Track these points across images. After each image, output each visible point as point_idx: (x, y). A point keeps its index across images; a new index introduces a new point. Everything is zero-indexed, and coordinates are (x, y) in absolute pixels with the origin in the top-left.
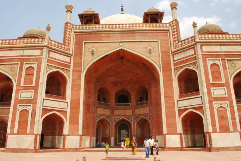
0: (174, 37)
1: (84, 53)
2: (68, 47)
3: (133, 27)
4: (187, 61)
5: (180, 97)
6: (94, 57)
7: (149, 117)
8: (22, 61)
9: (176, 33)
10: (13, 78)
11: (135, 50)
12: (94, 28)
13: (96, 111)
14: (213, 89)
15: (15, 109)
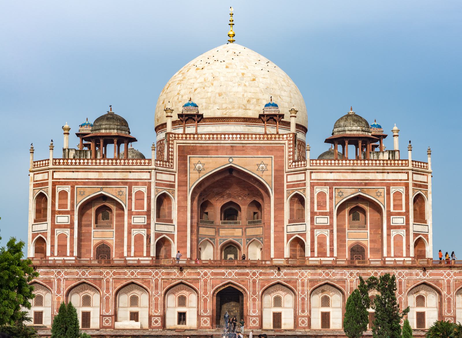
0: (289, 154)
1: (189, 170)
2: (172, 164)
3: (244, 138)
4: (298, 185)
5: (290, 222)
6: (201, 175)
7: (261, 239)
8: (130, 184)
9: (291, 150)
10: (123, 202)
11: (245, 168)
12: (200, 139)
13: (198, 231)
14: (316, 218)
15: (129, 233)
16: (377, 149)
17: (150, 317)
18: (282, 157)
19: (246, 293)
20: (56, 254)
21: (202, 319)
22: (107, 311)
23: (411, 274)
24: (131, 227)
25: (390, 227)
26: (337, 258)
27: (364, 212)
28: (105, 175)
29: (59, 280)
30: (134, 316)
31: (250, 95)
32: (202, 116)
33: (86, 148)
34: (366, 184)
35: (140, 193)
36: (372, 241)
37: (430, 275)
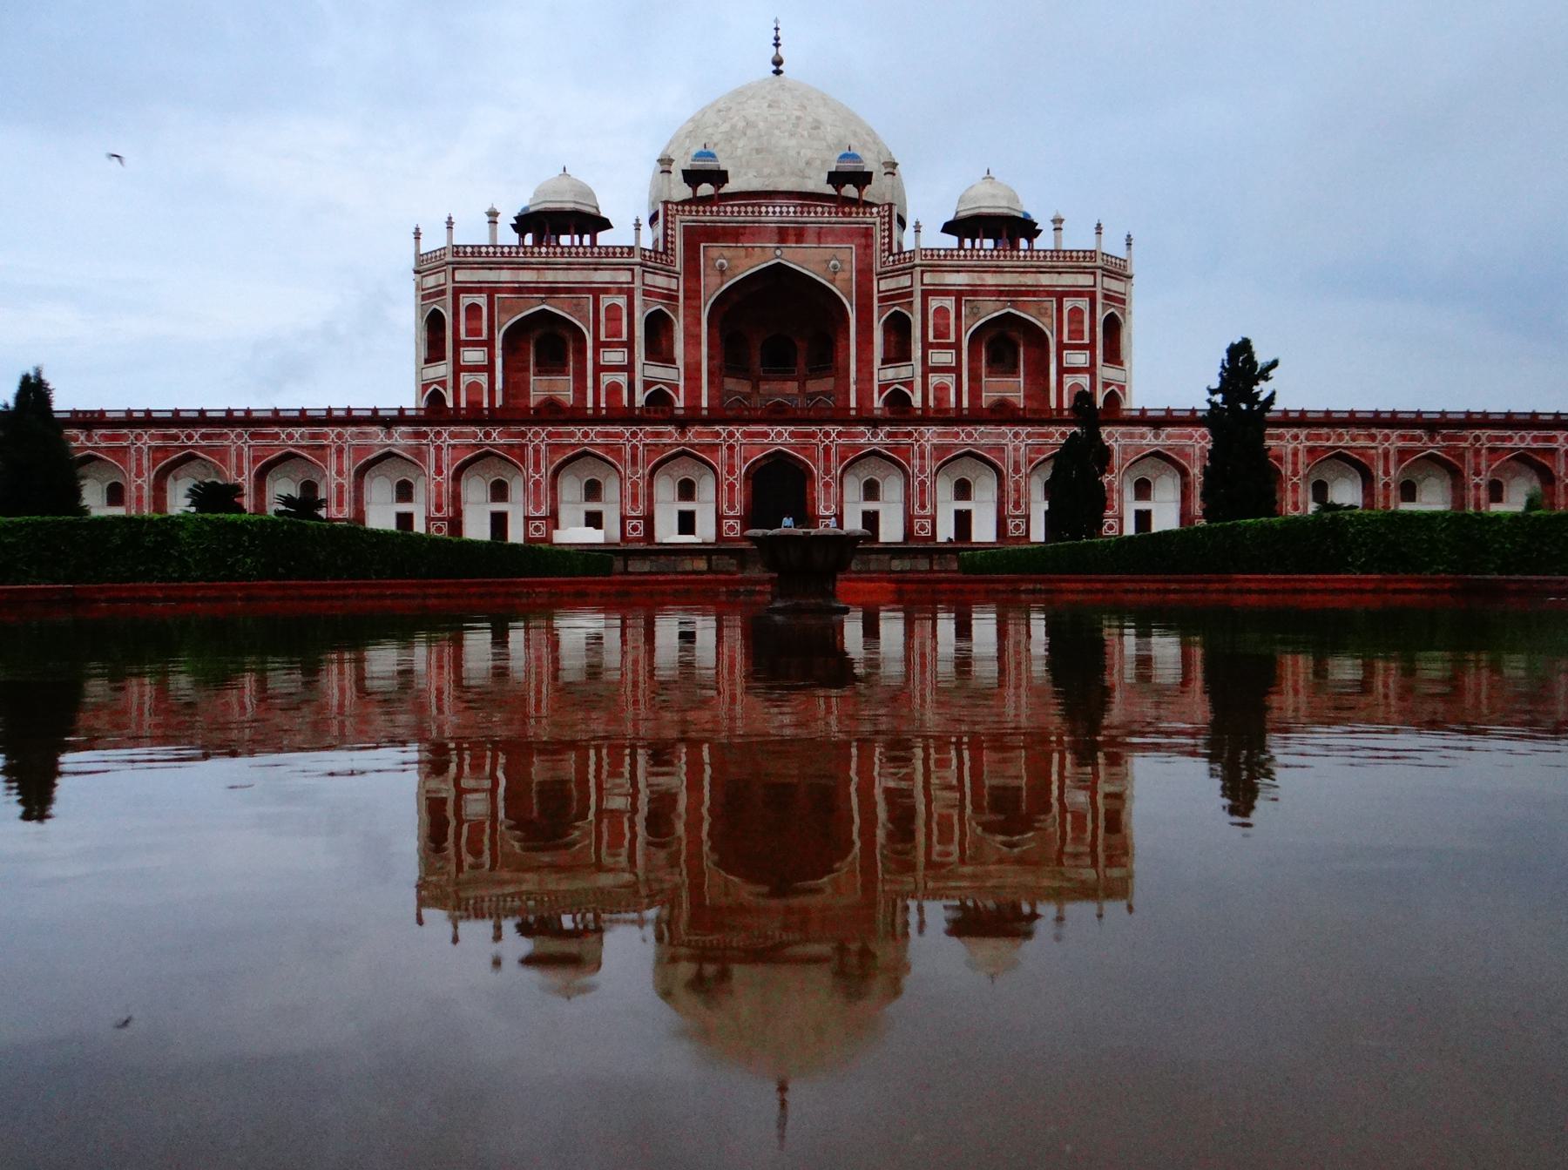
5: (884, 362)
8: (597, 292)
17: (623, 519)
18: (869, 246)
19: (811, 472)
21: (726, 523)
22: (537, 507)
23: (1131, 436)
24: (599, 369)
25: (1062, 371)
28: (550, 276)
30: (594, 520)
31: (807, 153)
35: (613, 309)
36: (1026, 397)
37: (1169, 437)
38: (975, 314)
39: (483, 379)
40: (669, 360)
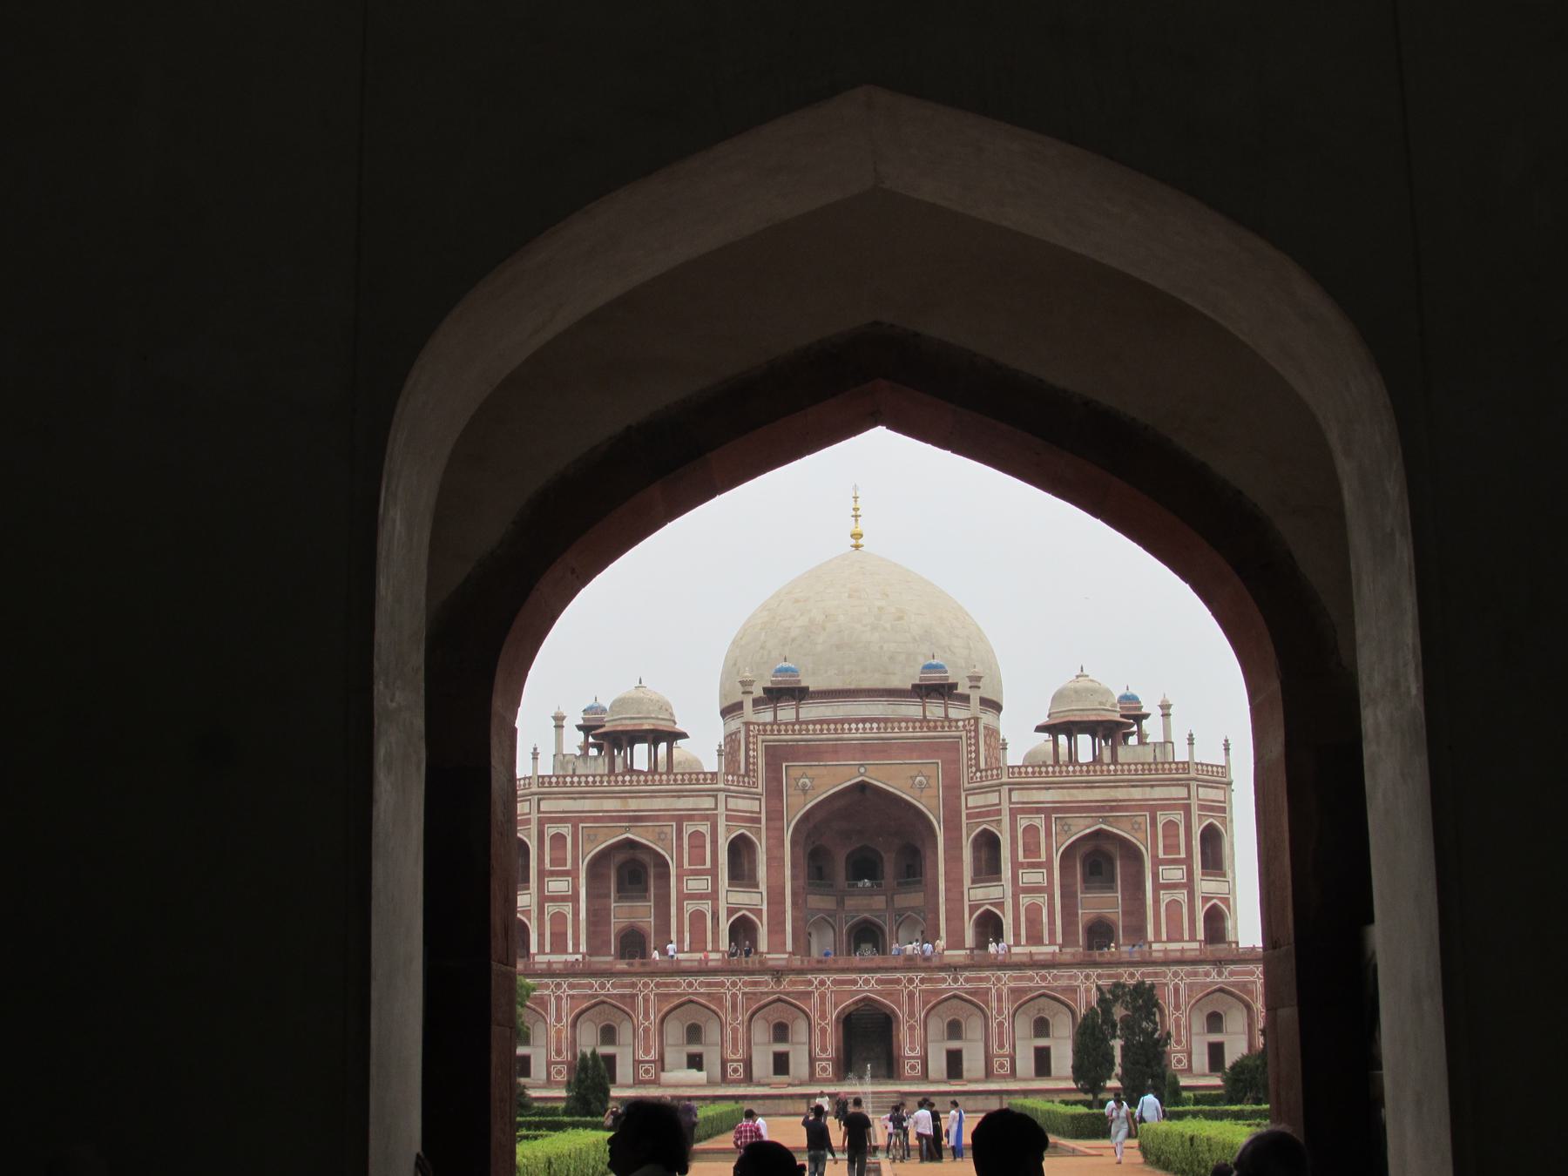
4: (988, 814)
5: (974, 882)
8: (680, 820)
13: (805, 901)
15: (680, 909)
16: (1133, 740)
17: (724, 1063)
18: (957, 761)
19: (896, 1016)
20: (548, 949)
22: (647, 1052)
23: (1196, 974)
24: (683, 897)
25: (1158, 887)
26: (1062, 947)
27: (1110, 861)
28: (633, 804)
29: (558, 998)
30: (695, 1062)
32: (807, 688)
33: (593, 752)
34: (1112, 809)
35: (697, 835)
37: (1232, 974)
38: (1067, 832)
39: (568, 909)
40: (753, 883)
